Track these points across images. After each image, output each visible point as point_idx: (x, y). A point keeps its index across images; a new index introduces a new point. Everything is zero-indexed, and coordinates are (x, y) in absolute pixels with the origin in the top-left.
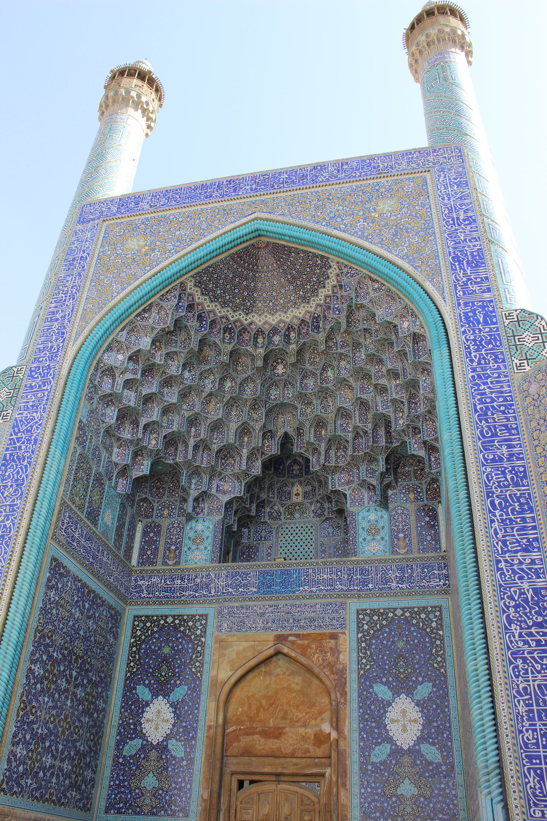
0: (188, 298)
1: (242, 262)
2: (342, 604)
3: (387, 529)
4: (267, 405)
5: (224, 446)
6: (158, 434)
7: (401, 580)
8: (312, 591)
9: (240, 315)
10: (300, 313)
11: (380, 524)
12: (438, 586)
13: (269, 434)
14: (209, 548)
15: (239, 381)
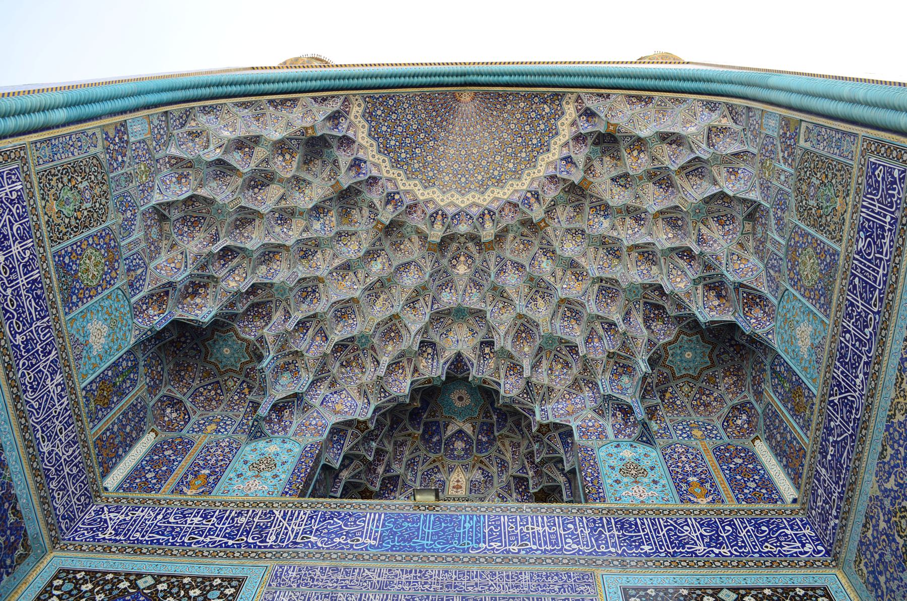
0: (348, 129)
1: (434, 114)
2: (583, 576)
3: (661, 471)
4: (435, 307)
5: (352, 339)
6: (245, 278)
7: (715, 541)
8: (508, 552)
9: (415, 185)
10: (505, 194)
11: (646, 463)
12: (801, 553)
13: (430, 350)
14: (283, 476)
15: (395, 264)
